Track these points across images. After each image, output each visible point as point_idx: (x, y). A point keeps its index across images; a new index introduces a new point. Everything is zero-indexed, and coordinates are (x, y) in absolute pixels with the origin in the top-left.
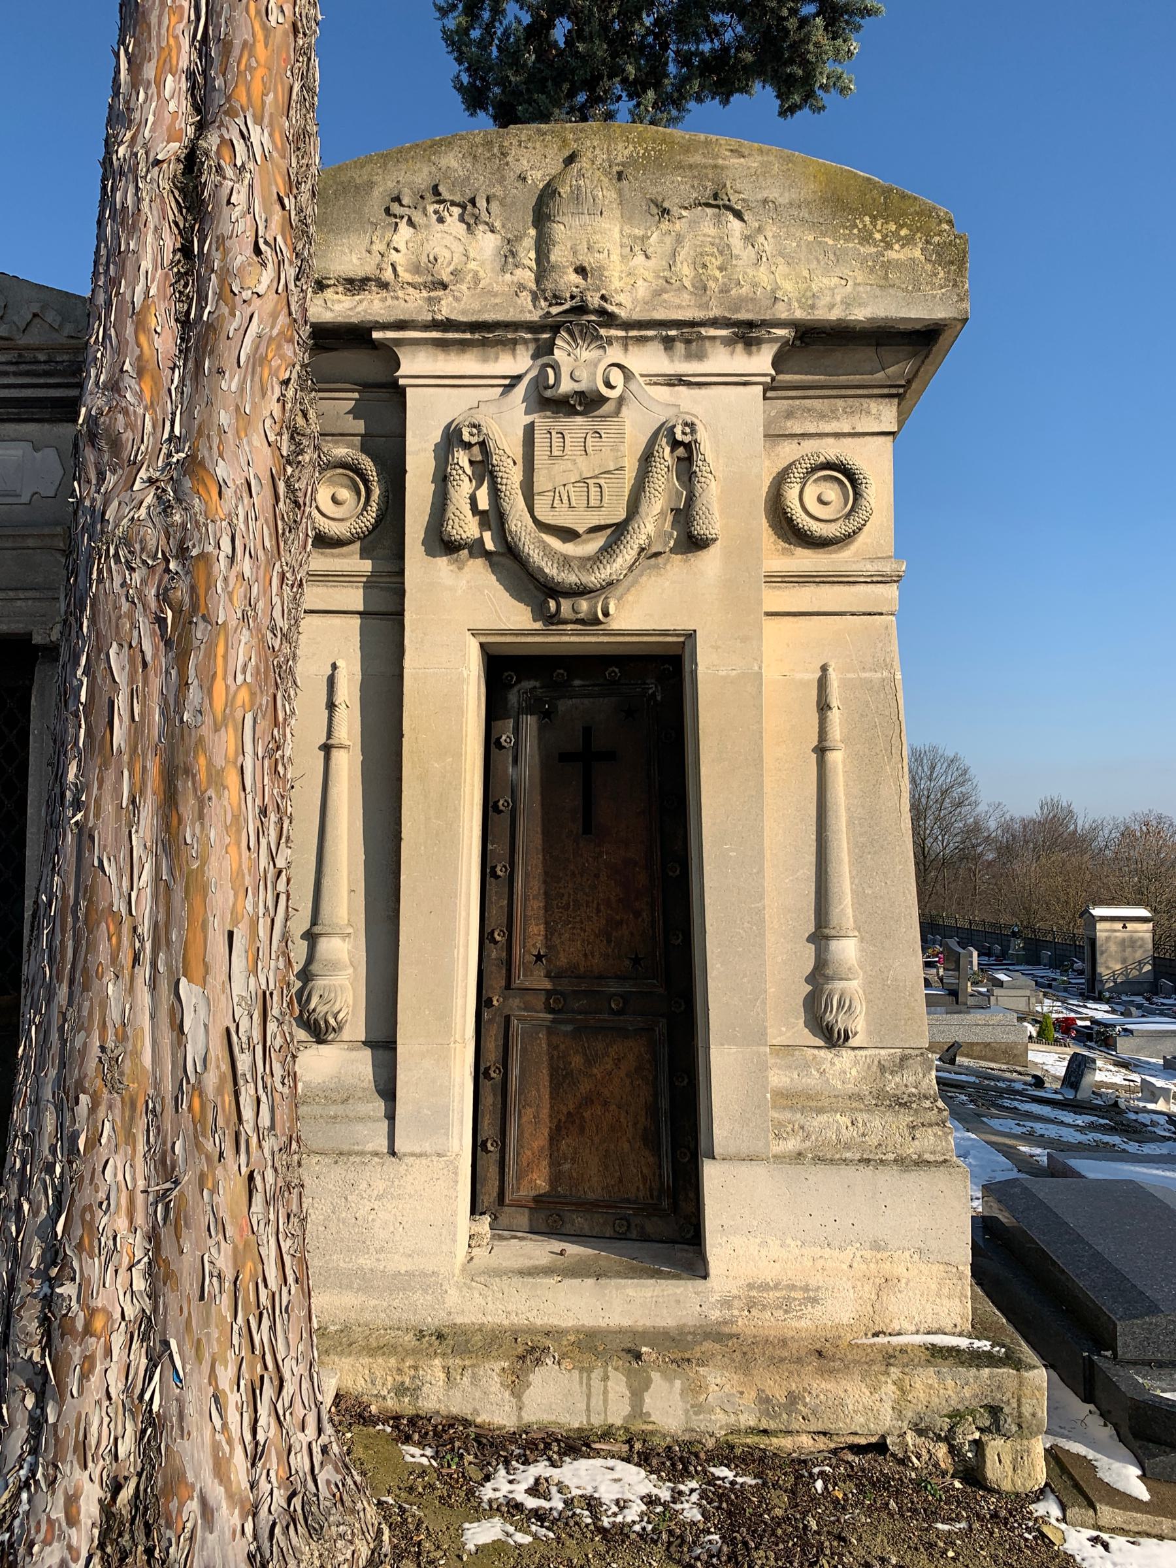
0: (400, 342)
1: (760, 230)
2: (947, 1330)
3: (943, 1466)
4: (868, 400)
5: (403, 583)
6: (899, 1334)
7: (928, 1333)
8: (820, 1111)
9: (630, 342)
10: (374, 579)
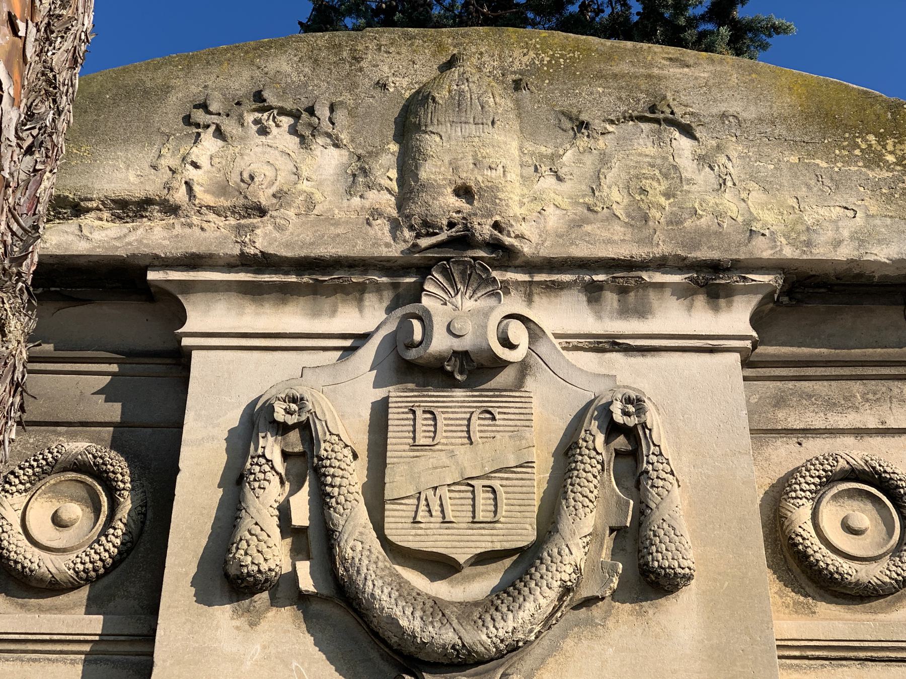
0: (189, 287)
1: (719, 148)
5: (151, 654)
10: (103, 647)
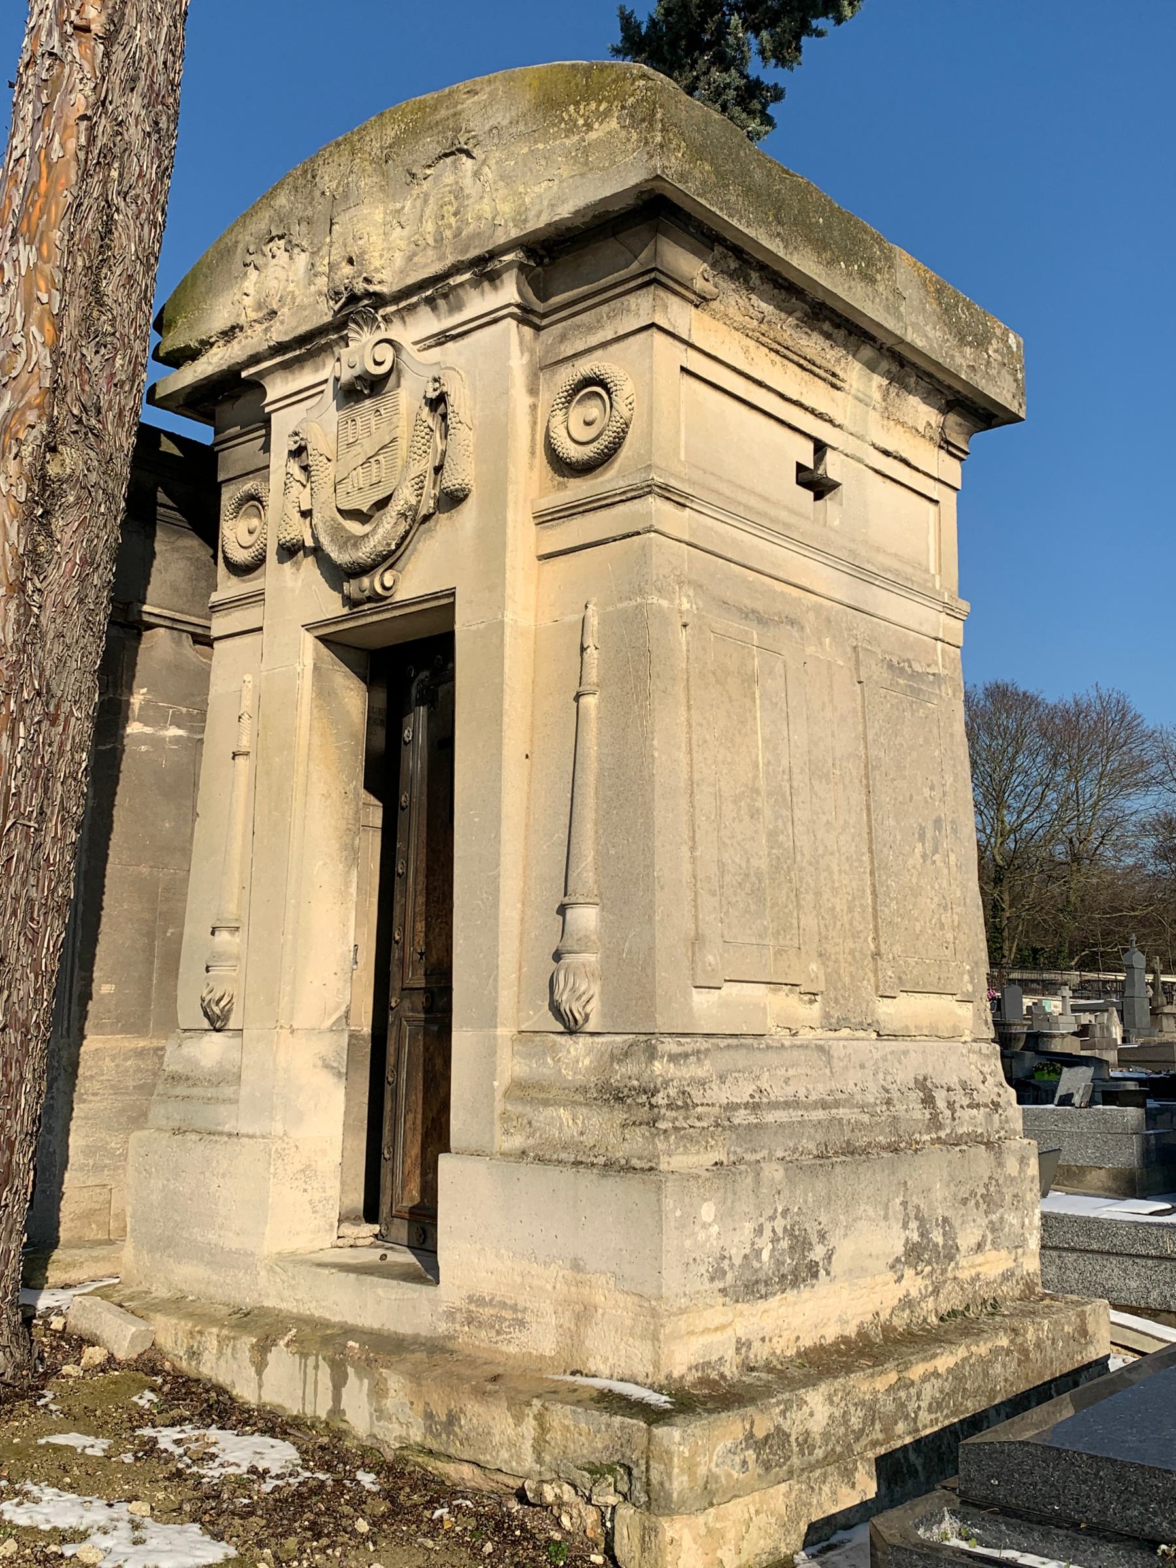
0: (262, 374)
1: (484, 162)
2: (639, 1380)
3: (590, 1533)
4: (627, 297)
6: (594, 1376)
7: (622, 1380)
8: (546, 1103)
9: (405, 314)
